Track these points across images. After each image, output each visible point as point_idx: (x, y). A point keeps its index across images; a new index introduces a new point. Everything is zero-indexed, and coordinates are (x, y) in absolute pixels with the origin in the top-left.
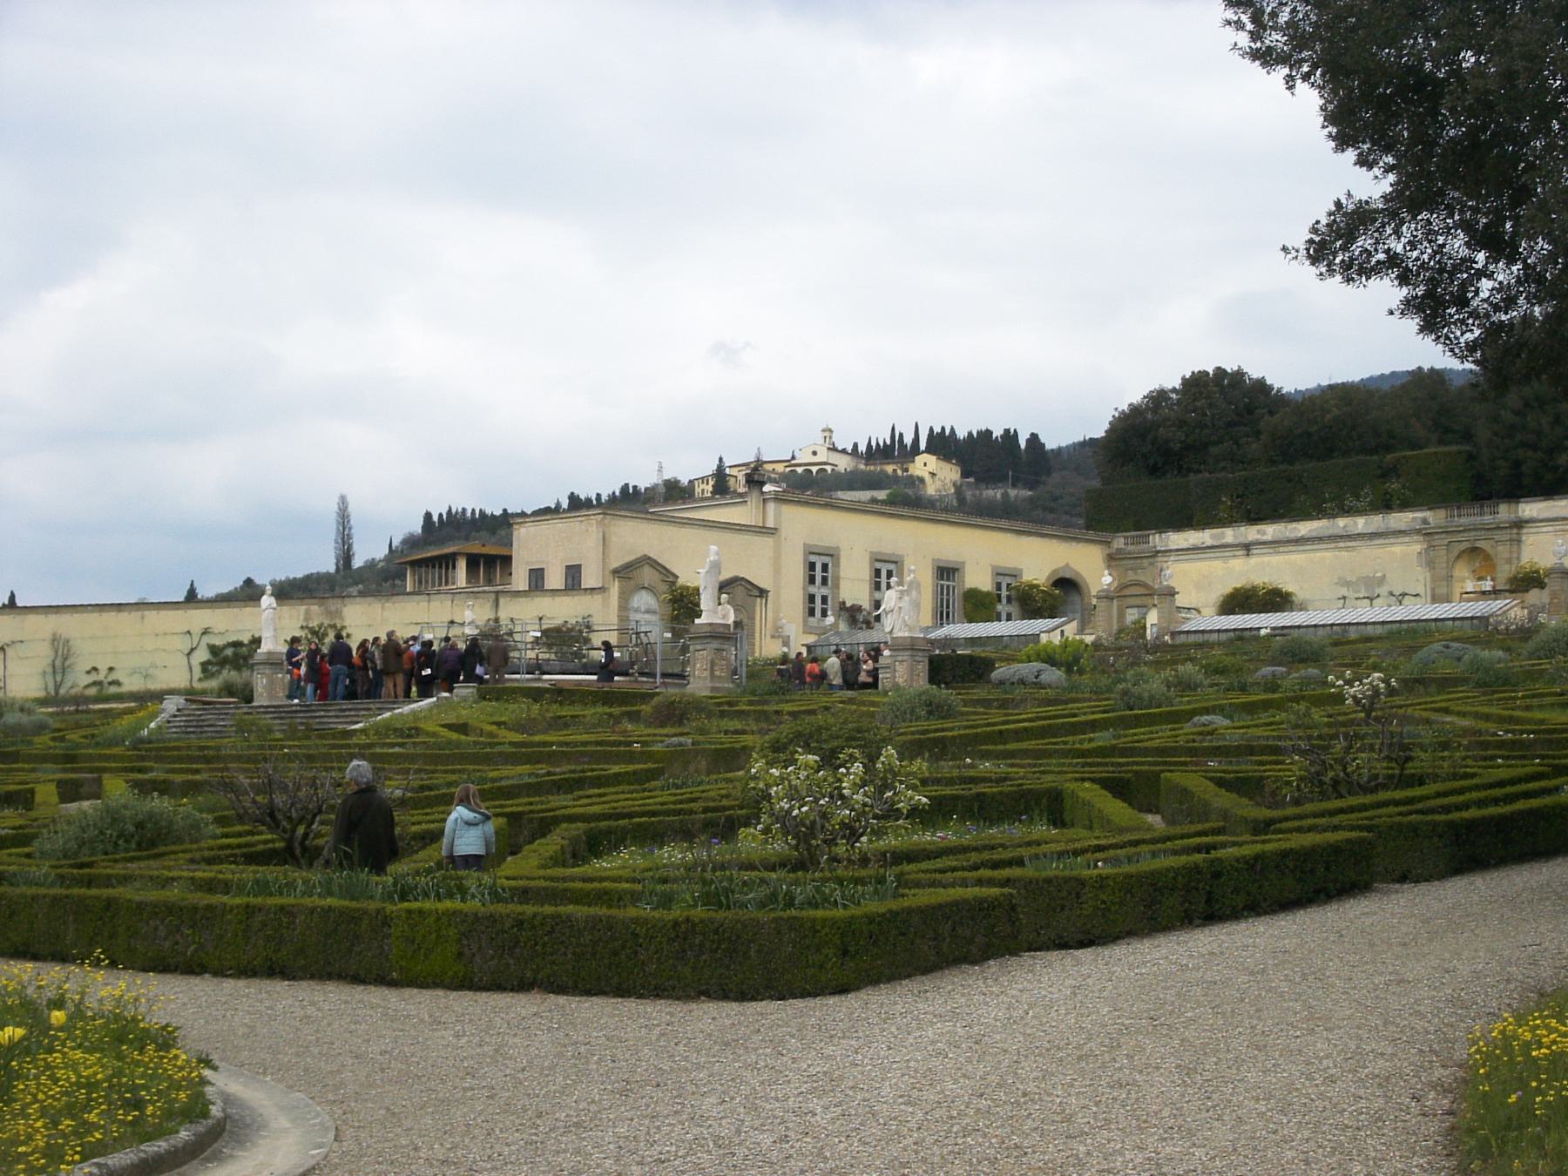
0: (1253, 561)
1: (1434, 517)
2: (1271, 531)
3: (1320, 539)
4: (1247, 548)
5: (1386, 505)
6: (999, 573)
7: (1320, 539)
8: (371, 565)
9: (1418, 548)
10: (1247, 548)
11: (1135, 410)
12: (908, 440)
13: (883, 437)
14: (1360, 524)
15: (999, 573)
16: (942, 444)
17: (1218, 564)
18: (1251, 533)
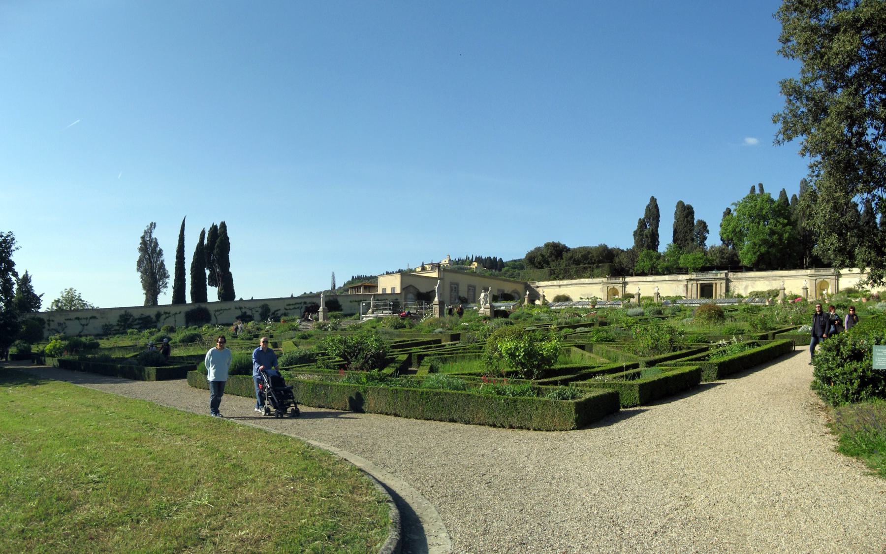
0: (561, 289)
1: (605, 280)
2: (565, 282)
3: (577, 284)
4: (560, 286)
5: (592, 276)
6: (499, 290)
7: (577, 284)
8: (340, 288)
9: (600, 287)
10: (560, 286)
11: (532, 252)
12: (470, 259)
13: (465, 258)
14: (587, 281)
15: (499, 290)
16: (479, 260)
17: (552, 290)
18: (561, 282)
